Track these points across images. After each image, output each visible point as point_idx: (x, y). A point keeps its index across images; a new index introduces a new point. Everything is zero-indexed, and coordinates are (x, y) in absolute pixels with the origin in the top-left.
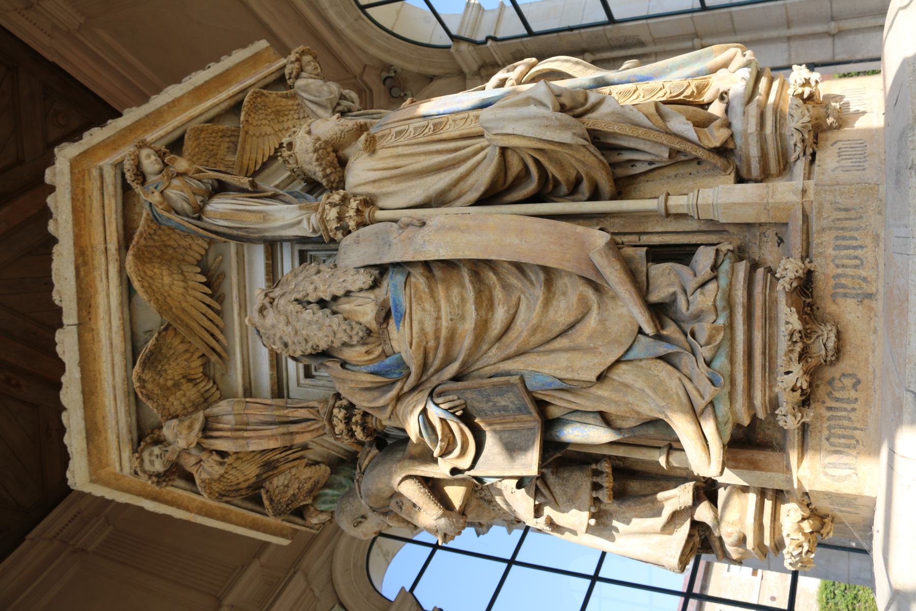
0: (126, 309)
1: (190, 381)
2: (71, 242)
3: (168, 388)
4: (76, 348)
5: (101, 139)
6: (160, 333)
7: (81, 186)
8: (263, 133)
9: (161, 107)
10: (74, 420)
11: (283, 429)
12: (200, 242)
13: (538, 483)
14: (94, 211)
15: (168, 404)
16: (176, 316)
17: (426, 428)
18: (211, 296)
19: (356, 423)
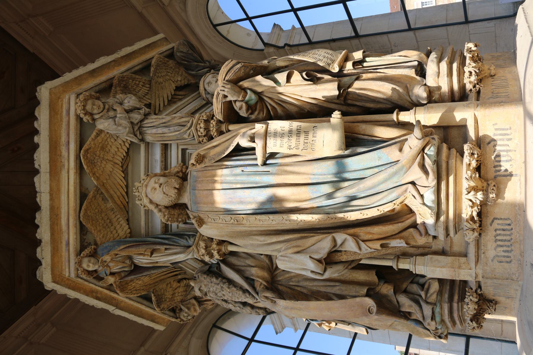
5: (50, 257)
6: (153, 293)
7: (65, 279)
8: (109, 173)
9: (50, 205)
15: (176, 301)
16: (154, 283)
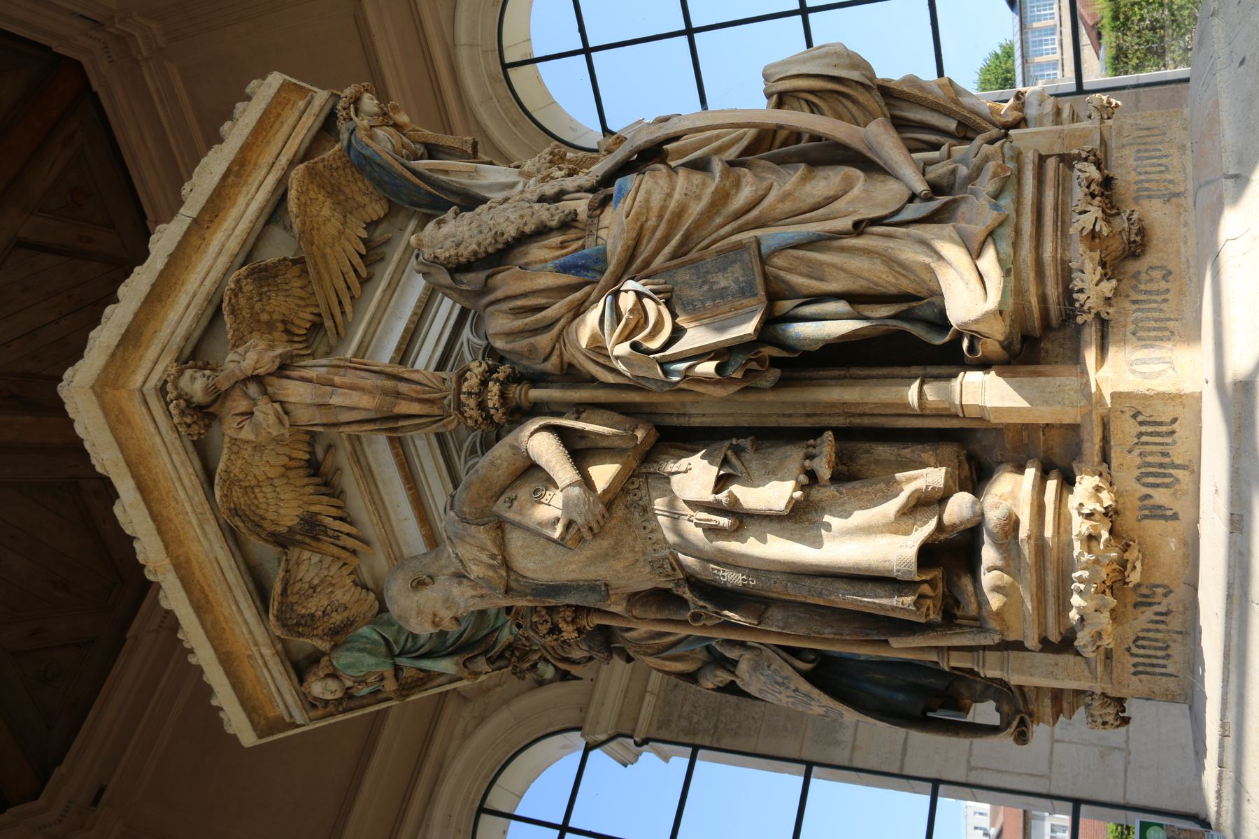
0: (262, 221)
1: (287, 331)
2: (239, 144)
3: (259, 321)
4: (178, 239)
10: (117, 318)
11: (389, 384)
12: (377, 207)
13: (729, 453)
14: (279, 134)
17: (611, 309)
18: (361, 256)
19: (497, 380)
